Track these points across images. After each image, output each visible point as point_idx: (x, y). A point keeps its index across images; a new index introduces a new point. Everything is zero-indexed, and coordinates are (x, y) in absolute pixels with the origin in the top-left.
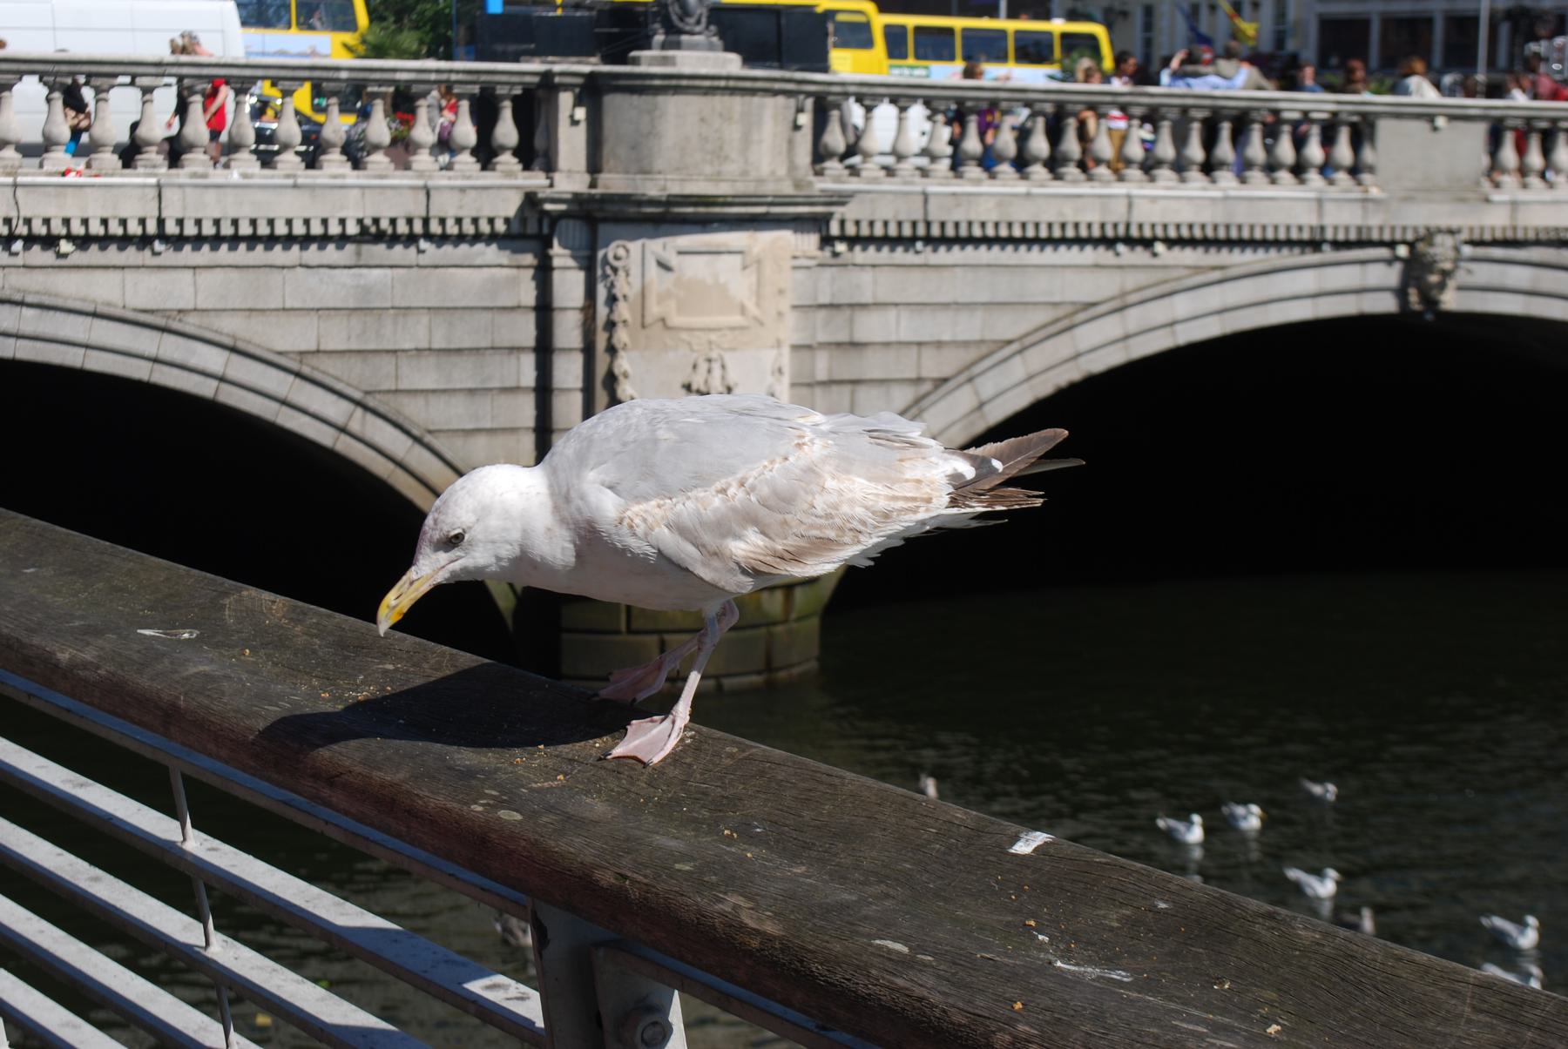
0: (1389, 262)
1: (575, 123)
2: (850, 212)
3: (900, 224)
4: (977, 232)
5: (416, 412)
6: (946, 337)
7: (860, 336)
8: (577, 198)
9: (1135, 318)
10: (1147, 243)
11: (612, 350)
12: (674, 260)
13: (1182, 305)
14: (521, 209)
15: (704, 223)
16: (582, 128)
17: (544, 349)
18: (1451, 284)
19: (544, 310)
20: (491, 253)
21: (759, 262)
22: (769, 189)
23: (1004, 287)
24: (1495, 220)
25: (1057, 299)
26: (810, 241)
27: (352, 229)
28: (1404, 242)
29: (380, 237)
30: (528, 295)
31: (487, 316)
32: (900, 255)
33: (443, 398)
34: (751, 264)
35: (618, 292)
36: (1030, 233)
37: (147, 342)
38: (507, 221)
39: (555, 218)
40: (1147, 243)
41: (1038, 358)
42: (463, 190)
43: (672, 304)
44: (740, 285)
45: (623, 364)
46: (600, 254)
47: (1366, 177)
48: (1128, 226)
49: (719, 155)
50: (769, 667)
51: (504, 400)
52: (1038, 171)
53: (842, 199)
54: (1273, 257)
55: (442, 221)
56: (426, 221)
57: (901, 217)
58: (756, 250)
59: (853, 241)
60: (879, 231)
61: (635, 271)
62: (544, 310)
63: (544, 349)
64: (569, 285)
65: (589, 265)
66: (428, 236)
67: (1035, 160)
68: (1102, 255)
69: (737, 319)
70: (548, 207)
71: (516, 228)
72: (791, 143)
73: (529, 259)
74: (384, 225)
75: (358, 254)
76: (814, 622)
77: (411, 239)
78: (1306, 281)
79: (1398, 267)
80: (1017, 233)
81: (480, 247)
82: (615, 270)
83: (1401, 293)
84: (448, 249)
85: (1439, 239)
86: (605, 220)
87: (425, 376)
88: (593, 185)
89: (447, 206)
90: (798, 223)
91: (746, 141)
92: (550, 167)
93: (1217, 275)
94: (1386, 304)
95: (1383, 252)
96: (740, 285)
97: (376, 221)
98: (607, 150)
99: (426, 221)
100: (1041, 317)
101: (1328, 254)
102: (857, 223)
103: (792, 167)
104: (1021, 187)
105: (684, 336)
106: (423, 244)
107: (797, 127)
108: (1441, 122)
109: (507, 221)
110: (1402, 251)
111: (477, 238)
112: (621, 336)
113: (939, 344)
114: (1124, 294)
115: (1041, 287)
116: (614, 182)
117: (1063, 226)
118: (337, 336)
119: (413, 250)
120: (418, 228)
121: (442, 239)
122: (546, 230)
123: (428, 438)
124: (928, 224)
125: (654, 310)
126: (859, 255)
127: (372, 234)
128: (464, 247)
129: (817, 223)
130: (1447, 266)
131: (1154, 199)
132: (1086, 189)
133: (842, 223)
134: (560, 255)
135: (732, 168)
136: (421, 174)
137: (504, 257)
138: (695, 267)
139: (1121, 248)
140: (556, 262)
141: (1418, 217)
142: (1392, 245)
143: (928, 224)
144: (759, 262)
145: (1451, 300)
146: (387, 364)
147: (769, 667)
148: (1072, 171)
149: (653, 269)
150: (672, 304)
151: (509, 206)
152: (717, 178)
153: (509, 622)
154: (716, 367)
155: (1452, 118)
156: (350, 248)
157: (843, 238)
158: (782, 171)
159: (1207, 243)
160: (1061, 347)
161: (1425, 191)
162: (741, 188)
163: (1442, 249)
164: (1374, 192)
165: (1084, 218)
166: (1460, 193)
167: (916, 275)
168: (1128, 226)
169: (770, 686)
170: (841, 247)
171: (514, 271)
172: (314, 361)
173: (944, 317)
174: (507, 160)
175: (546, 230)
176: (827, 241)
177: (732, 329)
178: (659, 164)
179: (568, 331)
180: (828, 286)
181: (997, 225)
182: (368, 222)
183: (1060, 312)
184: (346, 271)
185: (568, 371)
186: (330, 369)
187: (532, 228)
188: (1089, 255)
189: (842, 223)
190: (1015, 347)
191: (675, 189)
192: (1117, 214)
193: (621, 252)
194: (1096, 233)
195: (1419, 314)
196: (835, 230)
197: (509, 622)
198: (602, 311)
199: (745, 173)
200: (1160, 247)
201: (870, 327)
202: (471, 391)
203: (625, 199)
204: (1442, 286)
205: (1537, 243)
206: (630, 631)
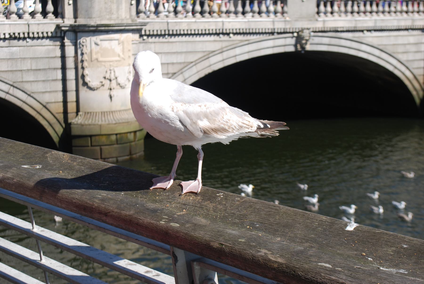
0: (292, 37)
1: (69, 5)
2: (147, 28)
3: (161, 31)
4: (182, 33)
5: (28, 87)
6: (175, 61)
8: (71, 26)
9: (225, 55)
10: (228, 34)
11: (83, 68)
12: (99, 42)
13: (238, 51)
14: (55, 29)
15: (107, 32)
16: (72, 6)
17: (64, 68)
18: (308, 43)
19: (63, 57)
20: (47, 42)
21: (123, 42)
22: (125, 22)
23: (190, 48)
24: (319, 25)
25: (204, 50)
26: (137, 36)
27: (7, 36)
28: (296, 32)
29: (15, 38)
30: (58, 53)
31: (47, 60)
32: (161, 39)
33: (36, 83)
34: (120, 43)
35: (84, 51)
36: (197, 32)
38: (52, 33)
39: (65, 32)
40: (228, 34)
41: (200, 66)
42: (38, 24)
43: (99, 55)
44: (118, 49)
45: (86, 72)
46: (78, 41)
47: (285, 15)
48: (223, 30)
49: (111, 13)
50: (131, 154)
51: (53, 83)
52: (198, 15)
53: (145, 24)
54: (262, 37)
55: (33, 33)
56: (28, 33)
57: (161, 29)
58: (122, 39)
59: (148, 36)
60: (155, 33)
61: (89, 46)
62: (63, 57)
63: (64, 68)
64: (70, 50)
65: (75, 45)
66: (29, 37)
67: (197, 12)
68: (216, 38)
69: (117, 58)
70: (63, 28)
71: (54, 35)
72: (130, 9)
73: (58, 43)
74: (17, 35)
75: (9, 43)
76: (142, 141)
77: (24, 38)
78: (270, 43)
79: (294, 39)
80: (193, 32)
81: (44, 40)
82: (83, 46)
83: (295, 46)
84: (35, 41)
85: (305, 31)
86: (79, 32)
87: (30, 77)
88: (75, 22)
89: (34, 29)
90: (133, 31)
91: (118, 9)
92: (63, 17)
93: (247, 42)
94: (291, 49)
95: (290, 35)
96: (118, 49)
97: (14, 34)
98: (79, 12)
99: (28, 33)
100: (200, 55)
101: (276, 36)
102: (149, 31)
103: (131, 16)
104: (194, 20)
105: (103, 63)
106: (28, 40)
107: (131, 5)
109: (52, 33)
111: (43, 38)
112: (85, 64)
113: (173, 64)
114: (222, 48)
115: (200, 47)
116: (81, 21)
117: (205, 30)
119: (25, 41)
120: (26, 35)
121: (33, 38)
122: (63, 35)
123: (32, 95)
124: (169, 31)
125: (94, 56)
126: (150, 40)
127: (13, 37)
128: (40, 40)
129: (138, 31)
130: (307, 38)
131: (229, 22)
132: (211, 20)
133: (145, 31)
134: (67, 42)
135: (114, 16)
136: (26, 20)
137: (51, 43)
138: (105, 44)
139: (221, 36)
140: (66, 44)
141: (299, 25)
142: (293, 33)
143: (169, 31)
144: (123, 42)
145: (309, 48)
146: (19, 74)
147: (131, 154)
148: (207, 15)
149: (93, 45)
150: (99, 55)
151: (52, 28)
152: (110, 19)
153: (58, 145)
154: (112, 72)
156: (7, 41)
157: (145, 35)
158: (128, 17)
159: (244, 34)
160: (206, 63)
161: (300, 18)
162: (117, 22)
163: (306, 34)
164: (288, 19)
165: (211, 28)
166: (310, 19)
167: (166, 45)
168: (223, 30)
169: (131, 159)
170: (145, 38)
171: (54, 47)
174: (51, 16)
175: (63, 35)
176: (141, 36)
177: (116, 61)
178: (94, 16)
179: (70, 63)
181: (187, 30)
182: (12, 34)
183: (205, 54)
184: (6, 48)
185: (71, 74)
187: (59, 35)
188: (213, 38)
189: (145, 31)
190: (194, 64)
191: (99, 23)
192: (220, 26)
193: (84, 41)
194: (214, 32)
195: (300, 51)
196: (143, 33)
197: (58, 145)
198: (80, 57)
199: (118, 18)
200: (231, 35)
202: (44, 81)
203: (85, 26)
204: (306, 44)
205: (330, 31)
206: (92, 146)
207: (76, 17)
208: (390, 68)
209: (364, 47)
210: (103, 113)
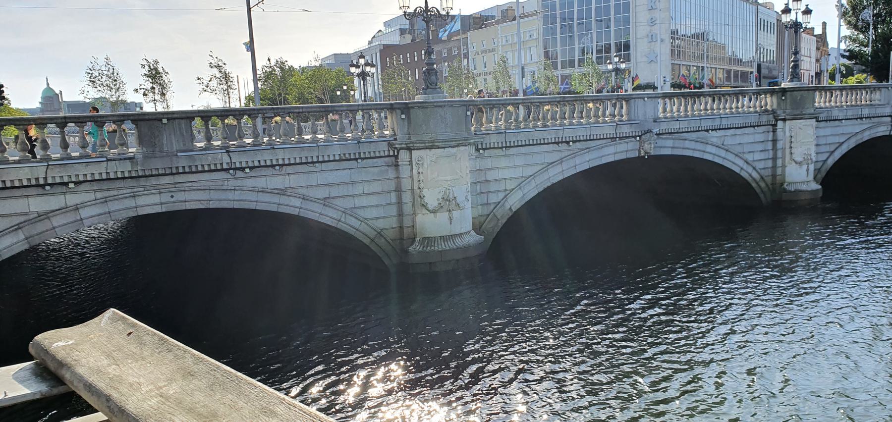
7: (489, 178)
9: (565, 166)
10: (568, 143)
13: (578, 160)
37: (276, 199)
78: (611, 149)
86: (414, 149)
108: (646, 99)
110: (638, 138)
113: (511, 179)
122: (396, 154)
155: (649, 98)
168: (562, 138)
170: (481, 151)
171: (387, 167)
172: (328, 201)
175: (396, 154)
176: (478, 150)
180: (480, 164)
183: (544, 166)
188: (551, 147)
201: (491, 175)
208: (737, 169)
209: (709, 148)
210: (444, 238)
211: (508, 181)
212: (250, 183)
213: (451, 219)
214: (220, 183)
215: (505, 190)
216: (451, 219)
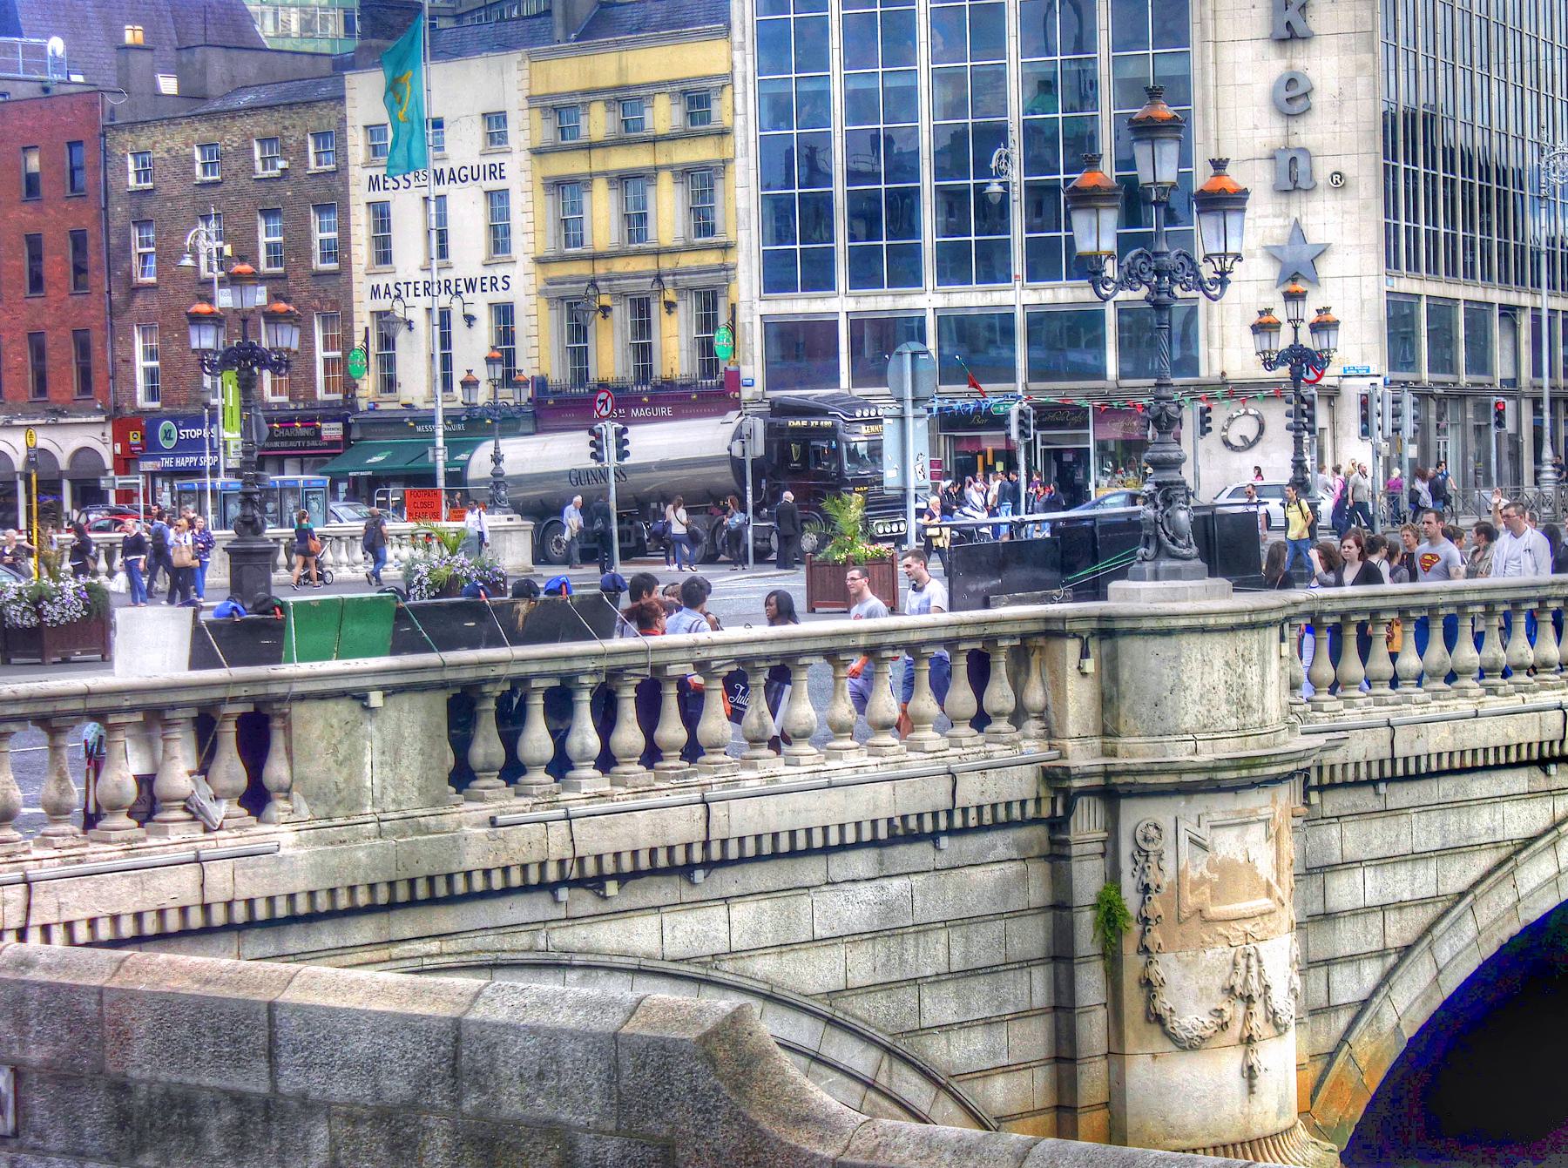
6: (1406, 896)
57: (1370, 758)
86: (1130, 795)
100: (1485, 861)
113: (1400, 906)
115: (1483, 823)
118: (862, 965)
173: (1403, 871)
175: (1060, 812)
184: (868, 885)
186: (860, 1008)
202: (988, 1022)
207: (1108, 731)
211: (1392, 916)
212: (608, 937)
213: (1250, 1073)
214: (523, 940)
215: (1382, 954)
216: (1250, 1073)
